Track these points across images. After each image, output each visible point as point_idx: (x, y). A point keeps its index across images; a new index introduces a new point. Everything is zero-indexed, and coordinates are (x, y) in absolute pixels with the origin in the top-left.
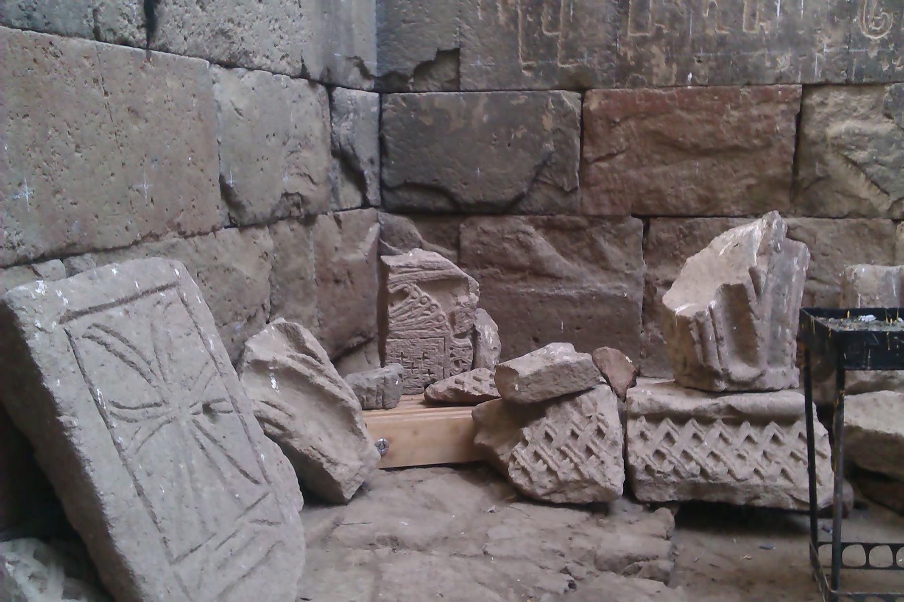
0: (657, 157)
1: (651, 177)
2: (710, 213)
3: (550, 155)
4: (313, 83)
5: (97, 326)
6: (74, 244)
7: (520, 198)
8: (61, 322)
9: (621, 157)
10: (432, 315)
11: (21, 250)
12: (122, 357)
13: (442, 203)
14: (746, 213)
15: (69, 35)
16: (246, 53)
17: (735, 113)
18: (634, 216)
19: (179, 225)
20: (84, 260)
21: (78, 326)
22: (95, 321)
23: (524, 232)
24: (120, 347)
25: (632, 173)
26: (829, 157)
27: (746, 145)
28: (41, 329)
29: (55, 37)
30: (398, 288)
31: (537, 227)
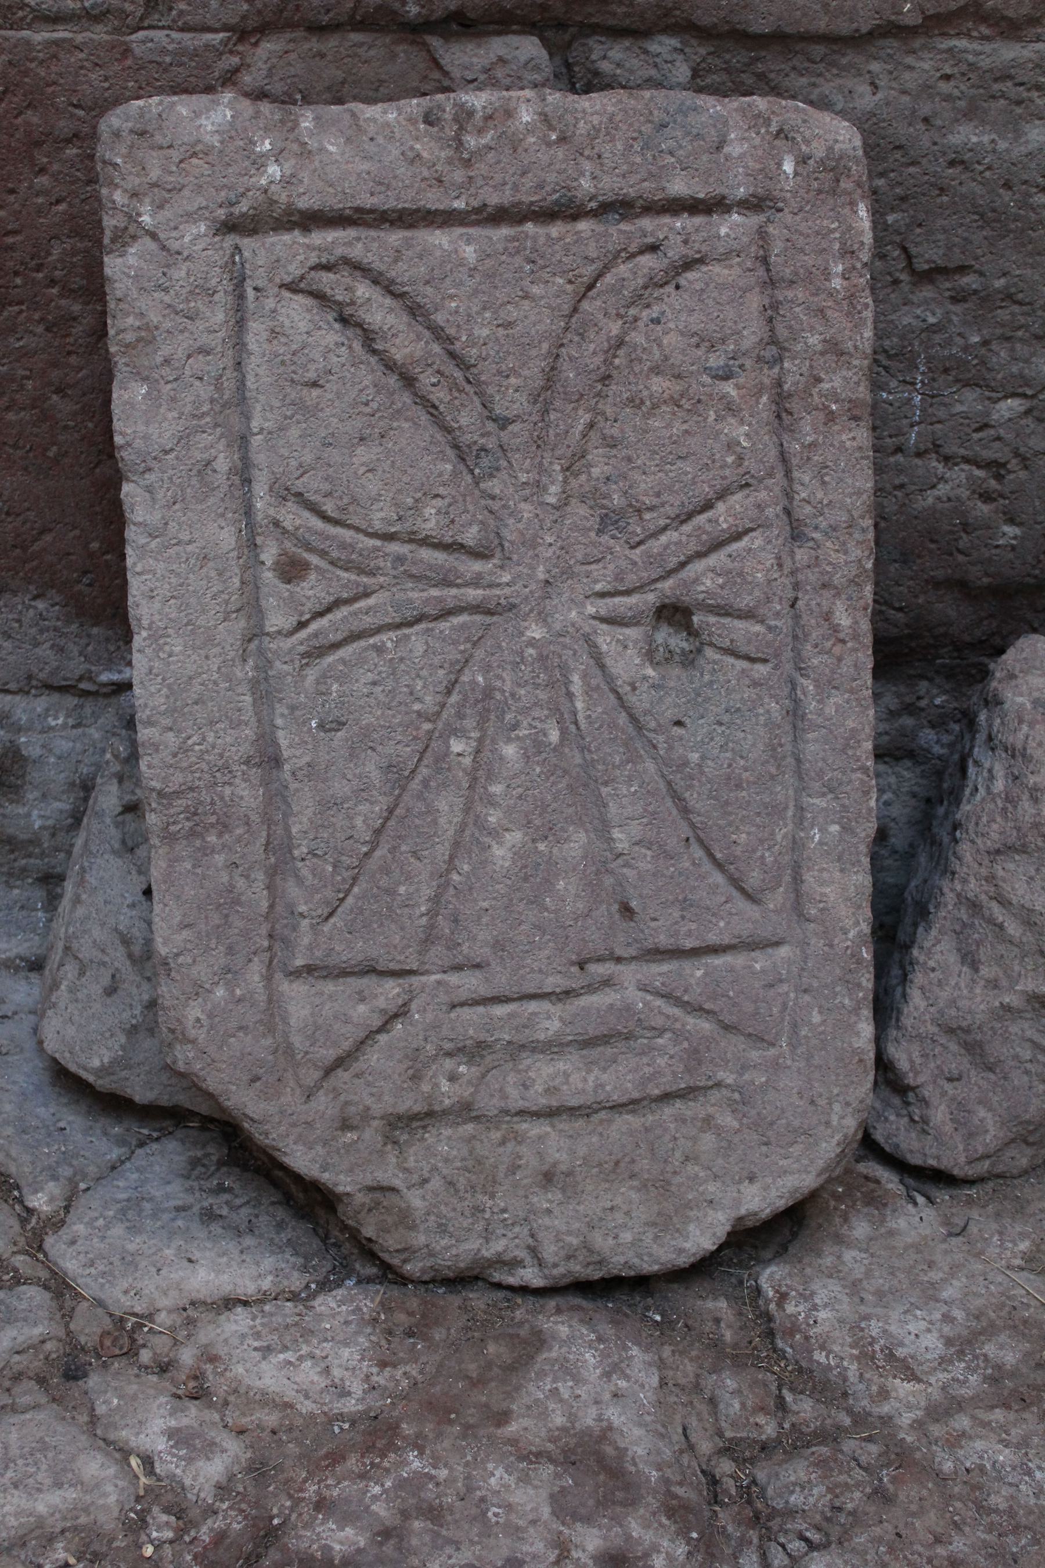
5: (358, 268)
8: (230, 227)
12: (409, 381)
20: (646, 52)
22: (356, 252)
28: (154, 236)
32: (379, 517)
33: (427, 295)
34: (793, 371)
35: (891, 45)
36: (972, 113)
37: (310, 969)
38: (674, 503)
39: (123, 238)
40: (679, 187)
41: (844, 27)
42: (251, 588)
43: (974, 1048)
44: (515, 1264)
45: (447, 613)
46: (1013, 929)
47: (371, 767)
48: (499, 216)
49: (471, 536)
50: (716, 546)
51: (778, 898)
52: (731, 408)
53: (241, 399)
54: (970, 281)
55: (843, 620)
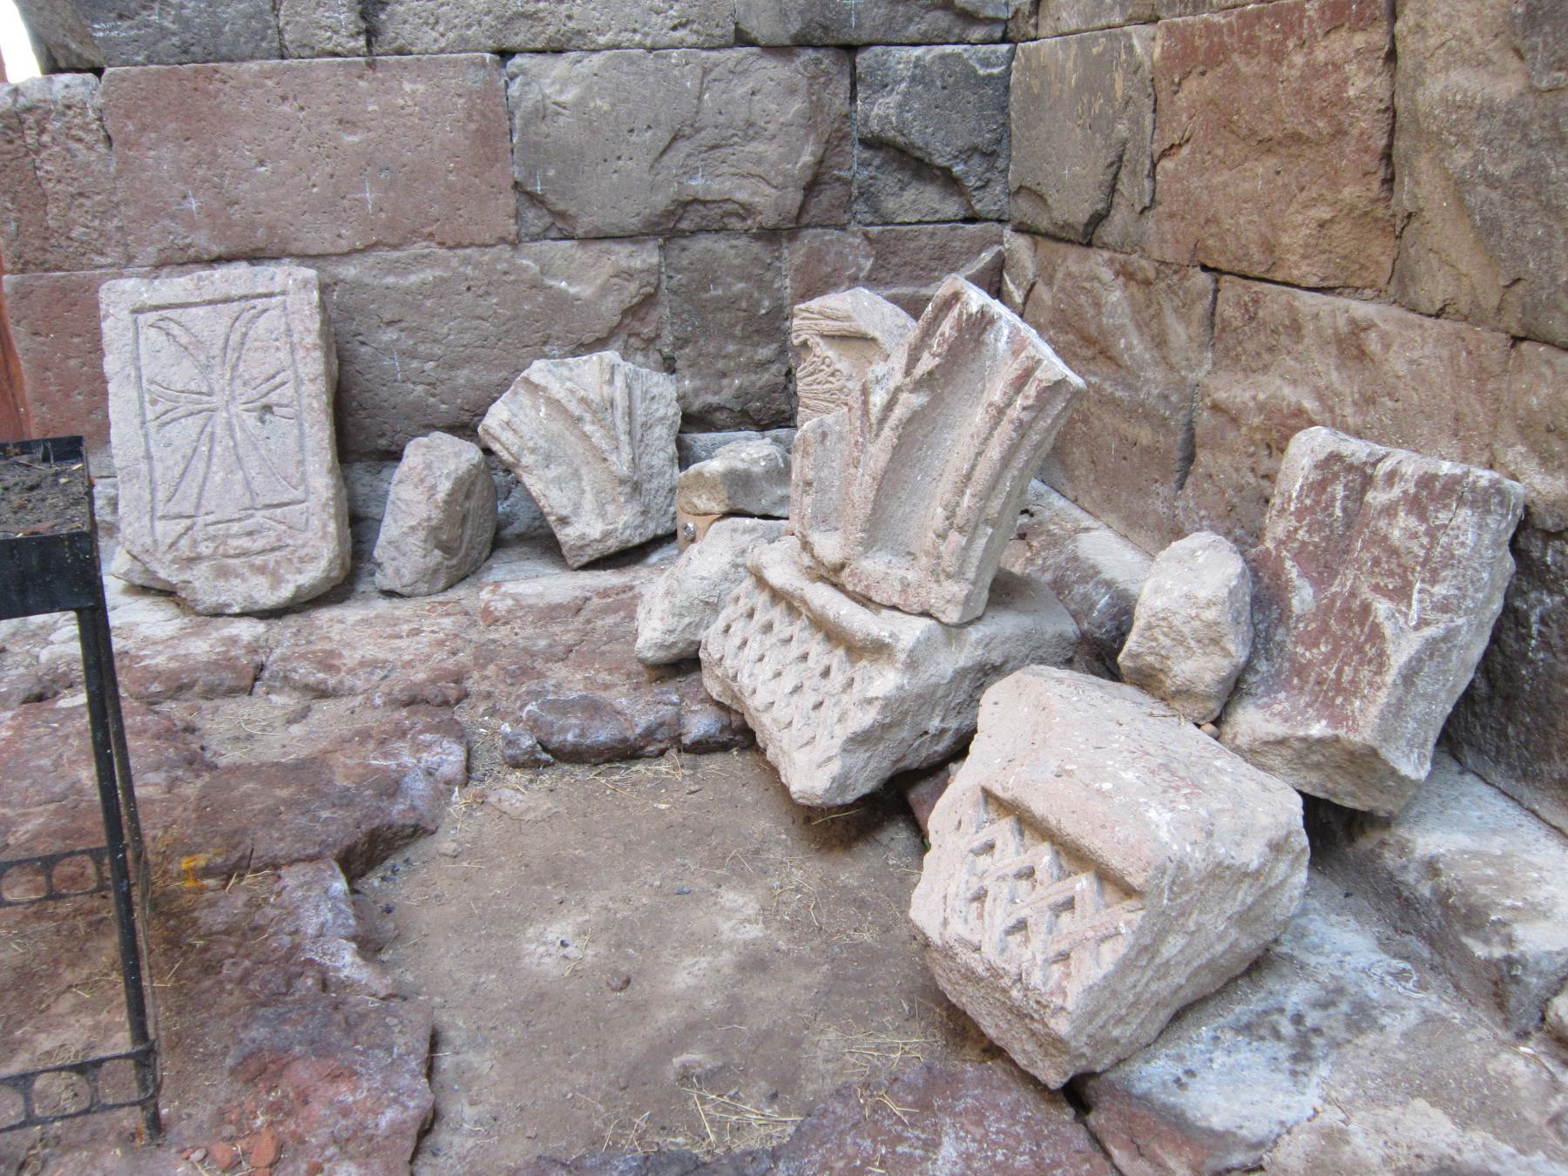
0: (1220, 151)
1: (1210, 189)
2: (1279, 276)
3: (1124, 143)
4: (774, 50)
6: (262, 249)
7: (1098, 219)
9: (1185, 151)
10: (837, 384)
11: (192, 252)
13: (1044, 223)
14: (1331, 283)
15: (243, 60)
16: (580, 33)
17: (1298, 59)
18: (1205, 268)
19: (431, 235)
21: (141, 318)
23: (1100, 281)
24: (184, 339)
25: (1195, 182)
26: (1423, 163)
27: (1306, 131)
29: (224, 65)
30: (801, 339)
31: (1117, 274)
32: (179, 386)
33: (190, 325)
34: (296, 338)
35: (358, 256)
36: (389, 272)
37: (163, 517)
38: (263, 377)
39: (106, 317)
40: (261, 290)
41: (339, 251)
42: (142, 407)
43: (397, 548)
44: (229, 606)
45: (200, 412)
46: (404, 507)
47: (178, 456)
48: (210, 303)
49: (205, 389)
50: (277, 387)
51: (302, 488)
52: (278, 349)
53: (138, 358)
54: (403, 325)
55: (315, 405)
